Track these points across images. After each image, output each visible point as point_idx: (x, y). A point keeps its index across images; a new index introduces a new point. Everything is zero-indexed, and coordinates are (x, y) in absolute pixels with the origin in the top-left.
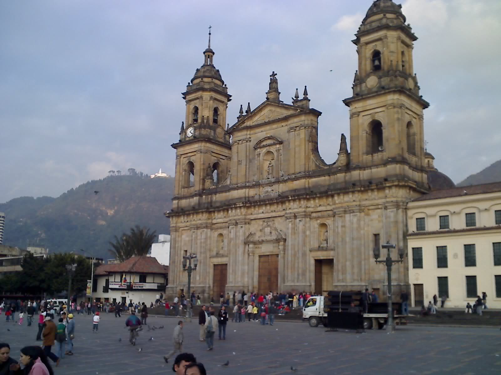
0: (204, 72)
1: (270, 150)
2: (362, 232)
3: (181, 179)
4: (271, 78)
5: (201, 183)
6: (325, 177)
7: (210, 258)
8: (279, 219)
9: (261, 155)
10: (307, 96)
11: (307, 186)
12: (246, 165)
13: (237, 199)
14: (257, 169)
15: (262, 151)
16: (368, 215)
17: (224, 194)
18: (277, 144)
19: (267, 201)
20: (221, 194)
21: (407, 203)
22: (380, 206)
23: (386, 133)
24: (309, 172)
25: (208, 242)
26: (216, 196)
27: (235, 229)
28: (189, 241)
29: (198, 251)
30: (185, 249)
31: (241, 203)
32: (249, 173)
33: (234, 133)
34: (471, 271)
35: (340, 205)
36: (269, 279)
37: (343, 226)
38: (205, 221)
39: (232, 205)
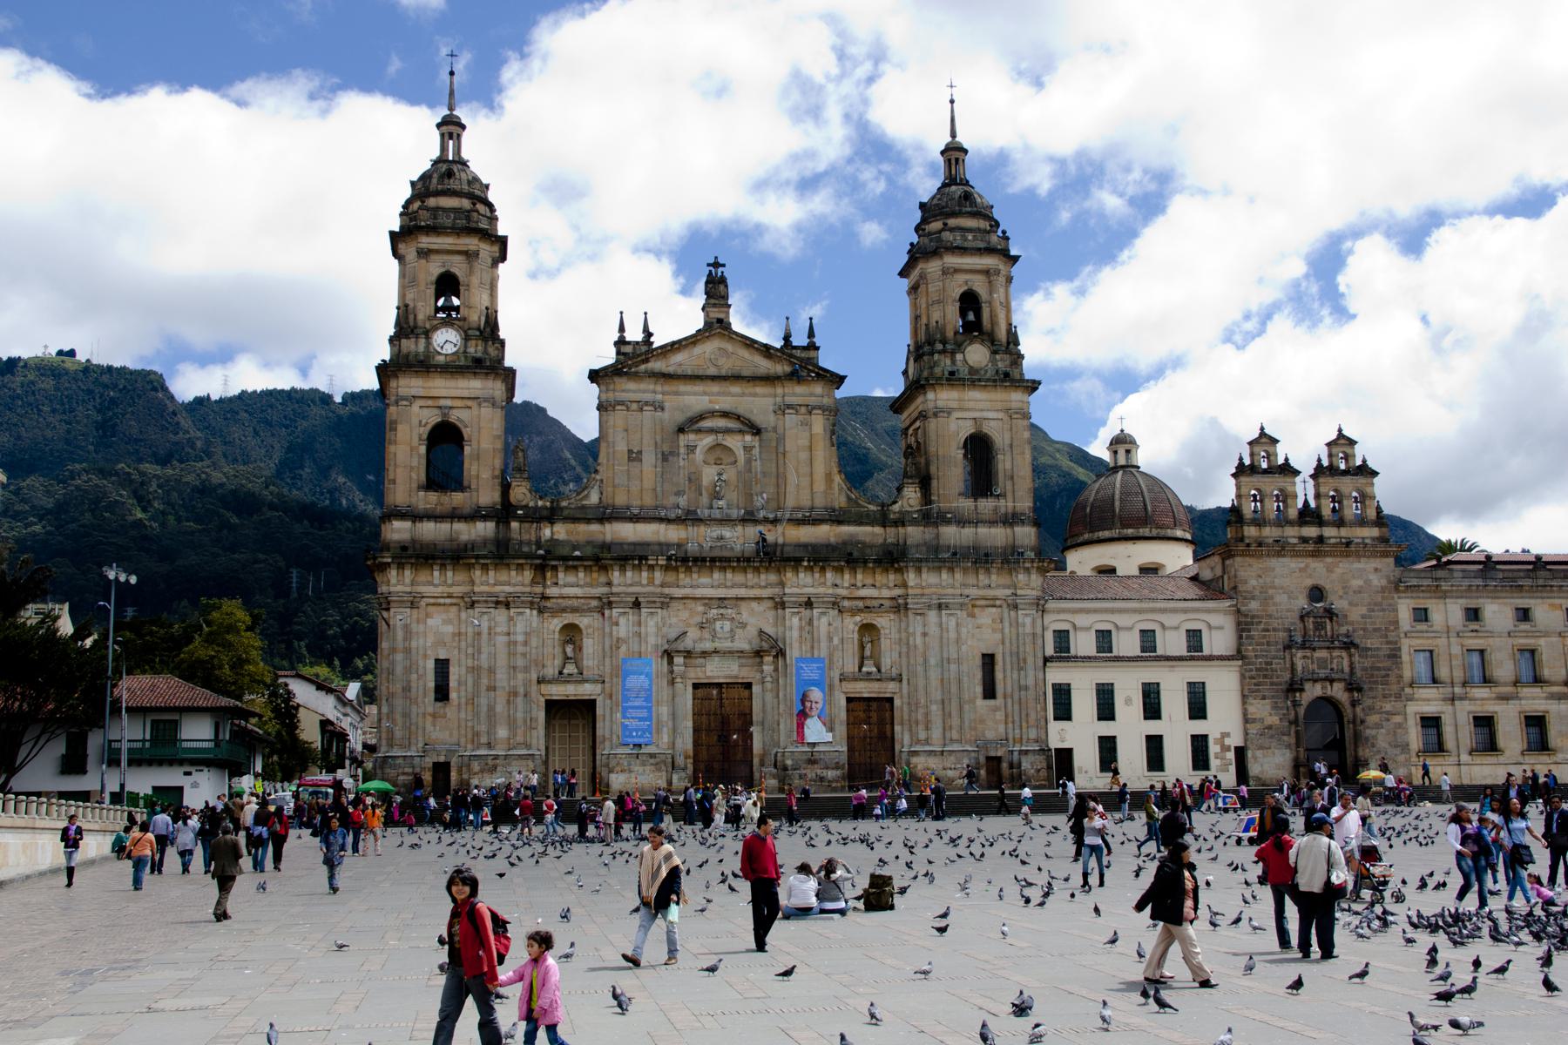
0: (469, 183)
1: (724, 443)
2: (964, 648)
3: (415, 463)
4: (710, 271)
5: (499, 488)
7: (539, 682)
8: (754, 604)
10: (814, 340)
11: (833, 540)
12: (656, 467)
13: (634, 544)
14: (690, 480)
15: (701, 440)
16: (972, 615)
17: (583, 528)
18: (748, 433)
20: (571, 526)
21: (1046, 601)
22: (998, 603)
23: (1003, 463)
24: (834, 510)
25: (534, 642)
26: (552, 527)
28: (454, 635)
29: (502, 661)
30: (441, 657)
32: (662, 487)
34: (1153, 727)
35: (919, 591)
36: (724, 738)
37: (925, 635)
38: (528, 589)
39: (633, 559)
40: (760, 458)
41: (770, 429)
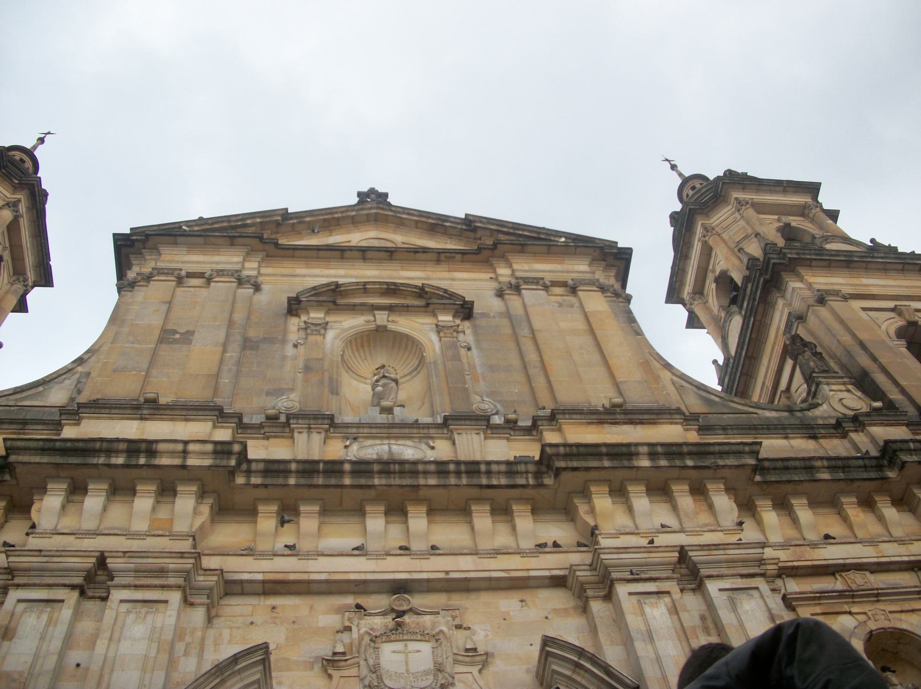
1: (391, 326)
6: (786, 438)
8: (508, 603)
9: (330, 334)
19: (426, 473)
27: (66, 613)
31: (209, 447)
33: (162, 249)
39: (109, 452)
40: (479, 348)
41: (492, 315)
